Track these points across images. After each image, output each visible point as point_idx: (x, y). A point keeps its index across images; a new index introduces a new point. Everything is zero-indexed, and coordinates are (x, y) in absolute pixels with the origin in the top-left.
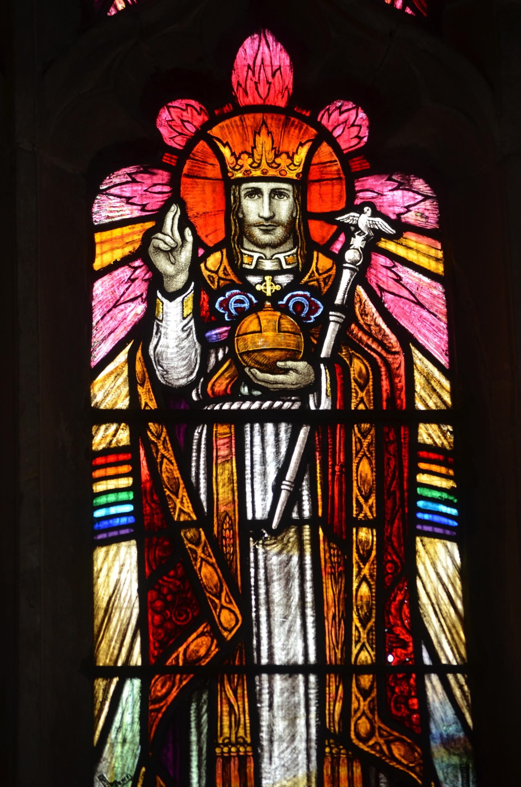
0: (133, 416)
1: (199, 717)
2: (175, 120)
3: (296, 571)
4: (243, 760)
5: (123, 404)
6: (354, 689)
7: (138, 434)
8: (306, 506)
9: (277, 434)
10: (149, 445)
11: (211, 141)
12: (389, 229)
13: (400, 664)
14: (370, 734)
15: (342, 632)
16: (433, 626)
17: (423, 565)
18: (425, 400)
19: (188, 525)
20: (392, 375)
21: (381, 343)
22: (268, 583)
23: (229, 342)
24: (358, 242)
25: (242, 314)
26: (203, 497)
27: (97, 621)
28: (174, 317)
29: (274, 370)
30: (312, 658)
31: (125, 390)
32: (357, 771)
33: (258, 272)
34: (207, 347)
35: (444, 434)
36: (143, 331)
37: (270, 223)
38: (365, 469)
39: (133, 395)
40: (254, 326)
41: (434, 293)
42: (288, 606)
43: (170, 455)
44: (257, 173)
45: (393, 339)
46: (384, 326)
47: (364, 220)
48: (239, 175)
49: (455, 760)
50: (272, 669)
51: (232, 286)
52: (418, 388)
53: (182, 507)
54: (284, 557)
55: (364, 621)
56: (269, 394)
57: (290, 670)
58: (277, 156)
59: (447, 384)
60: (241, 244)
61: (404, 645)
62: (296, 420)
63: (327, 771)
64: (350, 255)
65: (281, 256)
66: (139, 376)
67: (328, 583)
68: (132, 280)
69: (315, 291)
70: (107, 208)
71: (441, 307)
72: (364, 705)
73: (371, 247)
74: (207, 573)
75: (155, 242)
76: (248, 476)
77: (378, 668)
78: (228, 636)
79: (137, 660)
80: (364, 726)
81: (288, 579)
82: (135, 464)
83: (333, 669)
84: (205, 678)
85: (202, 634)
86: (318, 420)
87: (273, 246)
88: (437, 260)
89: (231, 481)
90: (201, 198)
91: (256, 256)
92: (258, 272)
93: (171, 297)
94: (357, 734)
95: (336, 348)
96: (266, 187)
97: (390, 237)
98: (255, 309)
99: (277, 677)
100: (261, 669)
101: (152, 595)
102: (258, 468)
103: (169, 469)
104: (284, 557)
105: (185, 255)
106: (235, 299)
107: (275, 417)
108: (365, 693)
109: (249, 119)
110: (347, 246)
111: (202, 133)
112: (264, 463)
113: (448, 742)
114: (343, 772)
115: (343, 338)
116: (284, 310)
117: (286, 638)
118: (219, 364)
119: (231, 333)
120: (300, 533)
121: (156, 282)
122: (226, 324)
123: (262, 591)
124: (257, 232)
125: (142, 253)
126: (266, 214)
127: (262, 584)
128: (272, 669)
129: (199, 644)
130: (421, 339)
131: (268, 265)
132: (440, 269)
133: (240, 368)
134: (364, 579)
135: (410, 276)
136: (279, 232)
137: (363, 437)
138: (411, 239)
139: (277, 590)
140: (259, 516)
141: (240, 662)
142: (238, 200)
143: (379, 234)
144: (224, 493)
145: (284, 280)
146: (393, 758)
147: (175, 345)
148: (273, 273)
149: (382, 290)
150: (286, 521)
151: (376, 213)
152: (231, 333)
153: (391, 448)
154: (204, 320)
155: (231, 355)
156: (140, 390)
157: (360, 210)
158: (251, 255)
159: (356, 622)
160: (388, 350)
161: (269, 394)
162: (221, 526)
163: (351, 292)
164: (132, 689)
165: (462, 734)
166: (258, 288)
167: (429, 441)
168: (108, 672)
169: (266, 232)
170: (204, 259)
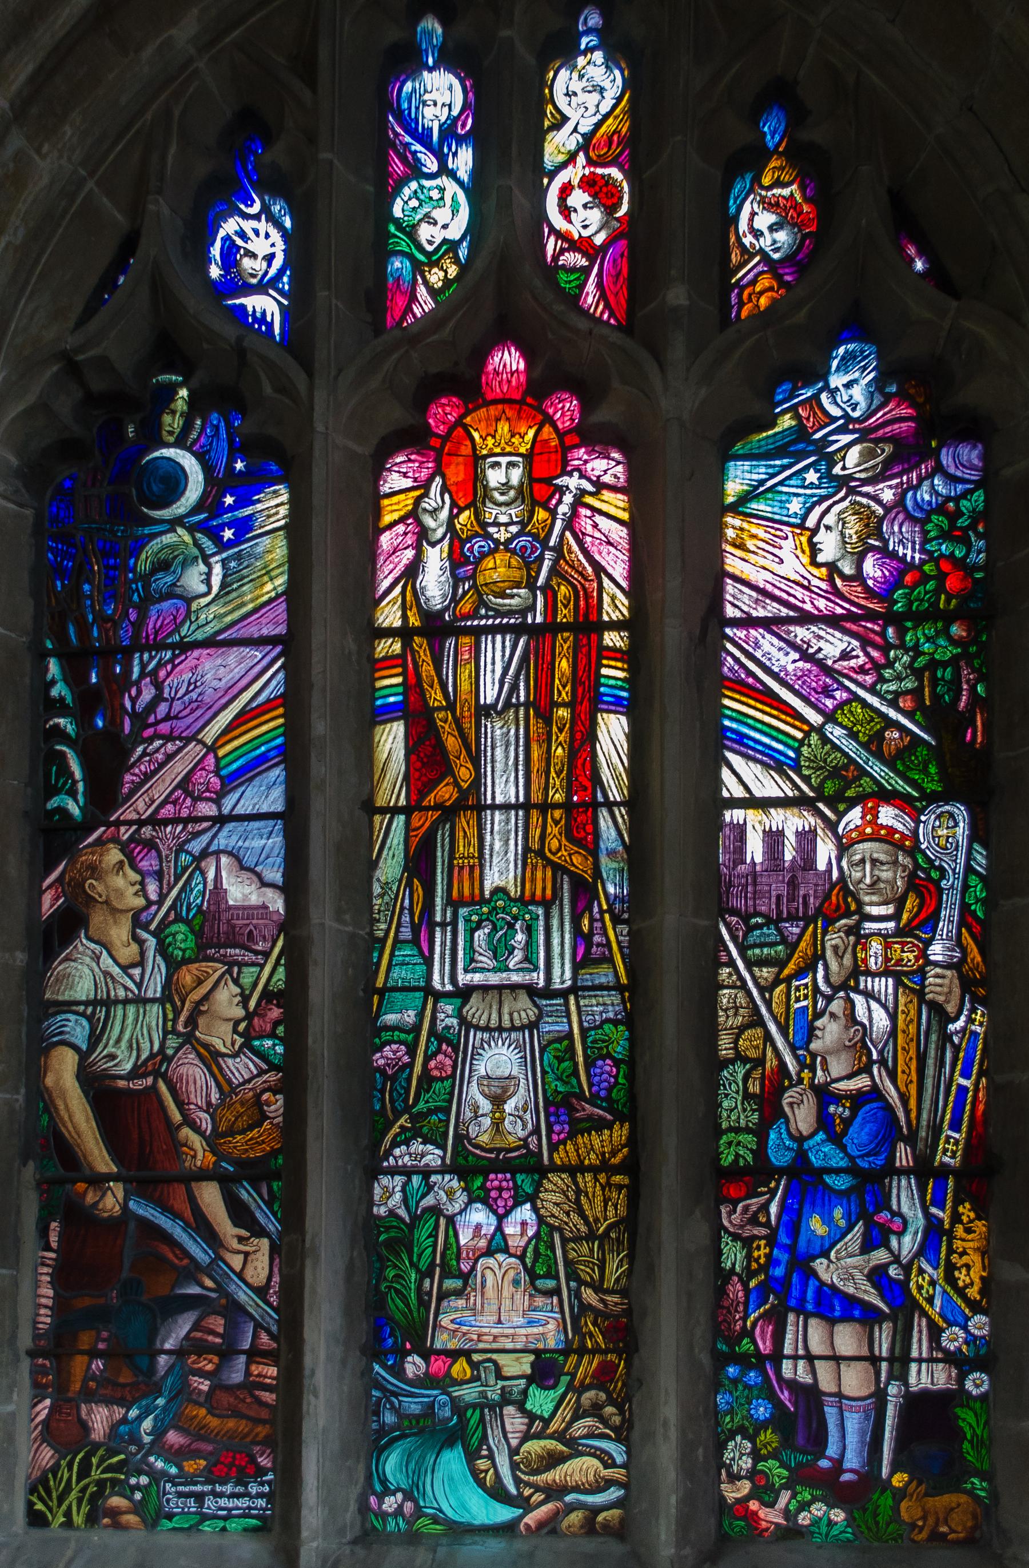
0: (404, 633)
1: (443, 840)
2: (442, 413)
3: (512, 740)
4: (472, 868)
5: (398, 623)
6: (549, 820)
7: (407, 645)
8: (522, 693)
9: (503, 643)
10: (413, 652)
11: (465, 427)
12: (590, 488)
13: (582, 803)
14: (559, 849)
15: (543, 781)
16: (606, 774)
17: (602, 735)
18: (609, 613)
19: (440, 709)
20: (588, 596)
21: (581, 574)
22: (493, 749)
23: (473, 577)
24: (568, 498)
25: (483, 555)
26: (450, 689)
27: (376, 777)
28: (435, 559)
29: (503, 595)
30: (521, 799)
31: (399, 614)
32: (549, 874)
33: (496, 524)
34: (457, 581)
35: (622, 638)
36: (413, 571)
37: (506, 486)
38: (564, 665)
39: (405, 617)
40: (491, 565)
41: (619, 533)
42: (506, 764)
43: (429, 659)
44: (498, 450)
45: (590, 570)
46: (584, 561)
47: (573, 482)
48: (484, 452)
49: (615, 865)
50: (494, 807)
51: (476, 535)
52: (605, 606)
53: (435, 697)
54: (505, 730)
55: (558, 774)
56: (499, 614)
57: (506, 807)
58: (513, 436)
59: (626, 602)
60: (484, 503)
61: (585, 789)
62: (517, 630)
63: (528, 874)
64: (563, 509)
65: (512, 512)
66: (408, 604)
67: (534, 746)
68: (405, 534)
69: (535, 537)
70: (394, 481)
71: (625, 544)
72: (556, 830)
73: (578, 503)
74: (452, 743)
75: (424, 505)
76: (482, 673)
77: (567, 806)
78: (465, 786)
79: (402, 802)
80: (555, 844)
81: (507, 745)
82: (404, 666)
83: (535, 806)
84: (449, 813)
85: (447, 784)
86: (532, 631)
87: (507, 504)
88: (624, 510)
89: (470, 676)
90: (456, 473)
91: (494, 512)
92: (496, 524)
93: (433, 545)
94: (550, 851)
95: (549, 579)
96: (504, 460)
97: (591, 494)
98: (492, 552)
99: (497, 813)
100: (487, 807)
101: (413, 757)
102: (489, 667)
103: (427, 669)
104: (505, 730)
105: (444, 514)
106: (479, 545)
107: (503, 630)
108: (556, 822)
109: (493, 411)
110: (560, 502)
111: (459, 422)
112: (493, 663)
113: (611, 854)
114: (539, 874)
115: (554, 571)
116: (513, 552)
117: (504, 787)
118: (465, 593)
119: (475, 570)
120: (517, 713)
121: (423, 535)
122: (471, 563)
123: (489, 754)
124: (496, 495)
125: (413, 514)
126: (504, 481)
127: (489, 749)
128: (494, 807)
129: (445, 792)
130: (610, 570)
131: (503, 519)
132: (625, 516)
133: (480, 595)
134: (560, 744)
135: (603, 522)
136: (512, 493)
137: (564, 642)
138: (607, 495)
139: (499, 753)
140: (488, 702)
141: (472, 802)
142: (483, 471)
143: (583, 492)
144: (465, 686)
145: (514, 529)
146: (573, 865)
147: (434, 581)
148: (506, 525)
149: (584, 534)
150: (508, 704)
151: (582, 476)
152: (475, 570)
153: (584, 650)
154: (457, 559)
155: (474, 586)
156: (409, 613)
157: (571, 475)
158: (491, 512)
159: (553, 774)
160: (586, 579)
161: (499, 614)
162: (462, 709)
163: (562, 536)
164: (400, 820)
165: (621, 848)
166: (495, 536)
167: (611, 644)
168: (383, 811)
169: (502, 494)
170: (457, 516)
